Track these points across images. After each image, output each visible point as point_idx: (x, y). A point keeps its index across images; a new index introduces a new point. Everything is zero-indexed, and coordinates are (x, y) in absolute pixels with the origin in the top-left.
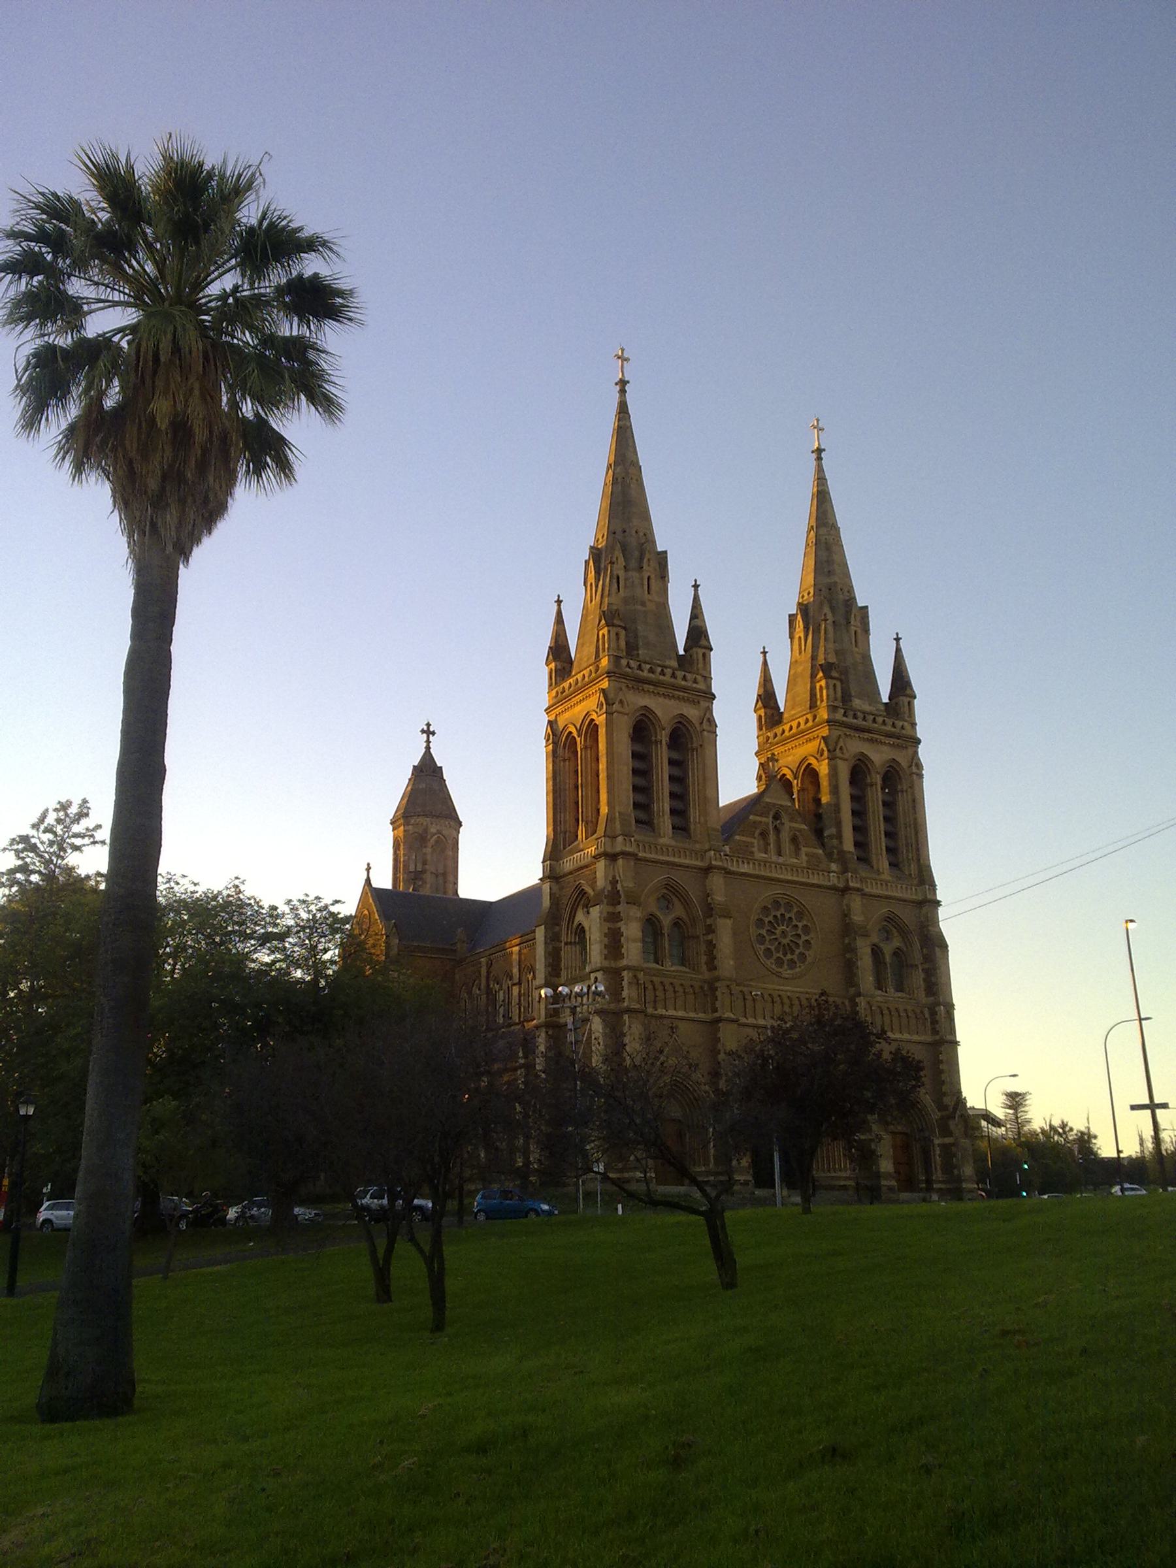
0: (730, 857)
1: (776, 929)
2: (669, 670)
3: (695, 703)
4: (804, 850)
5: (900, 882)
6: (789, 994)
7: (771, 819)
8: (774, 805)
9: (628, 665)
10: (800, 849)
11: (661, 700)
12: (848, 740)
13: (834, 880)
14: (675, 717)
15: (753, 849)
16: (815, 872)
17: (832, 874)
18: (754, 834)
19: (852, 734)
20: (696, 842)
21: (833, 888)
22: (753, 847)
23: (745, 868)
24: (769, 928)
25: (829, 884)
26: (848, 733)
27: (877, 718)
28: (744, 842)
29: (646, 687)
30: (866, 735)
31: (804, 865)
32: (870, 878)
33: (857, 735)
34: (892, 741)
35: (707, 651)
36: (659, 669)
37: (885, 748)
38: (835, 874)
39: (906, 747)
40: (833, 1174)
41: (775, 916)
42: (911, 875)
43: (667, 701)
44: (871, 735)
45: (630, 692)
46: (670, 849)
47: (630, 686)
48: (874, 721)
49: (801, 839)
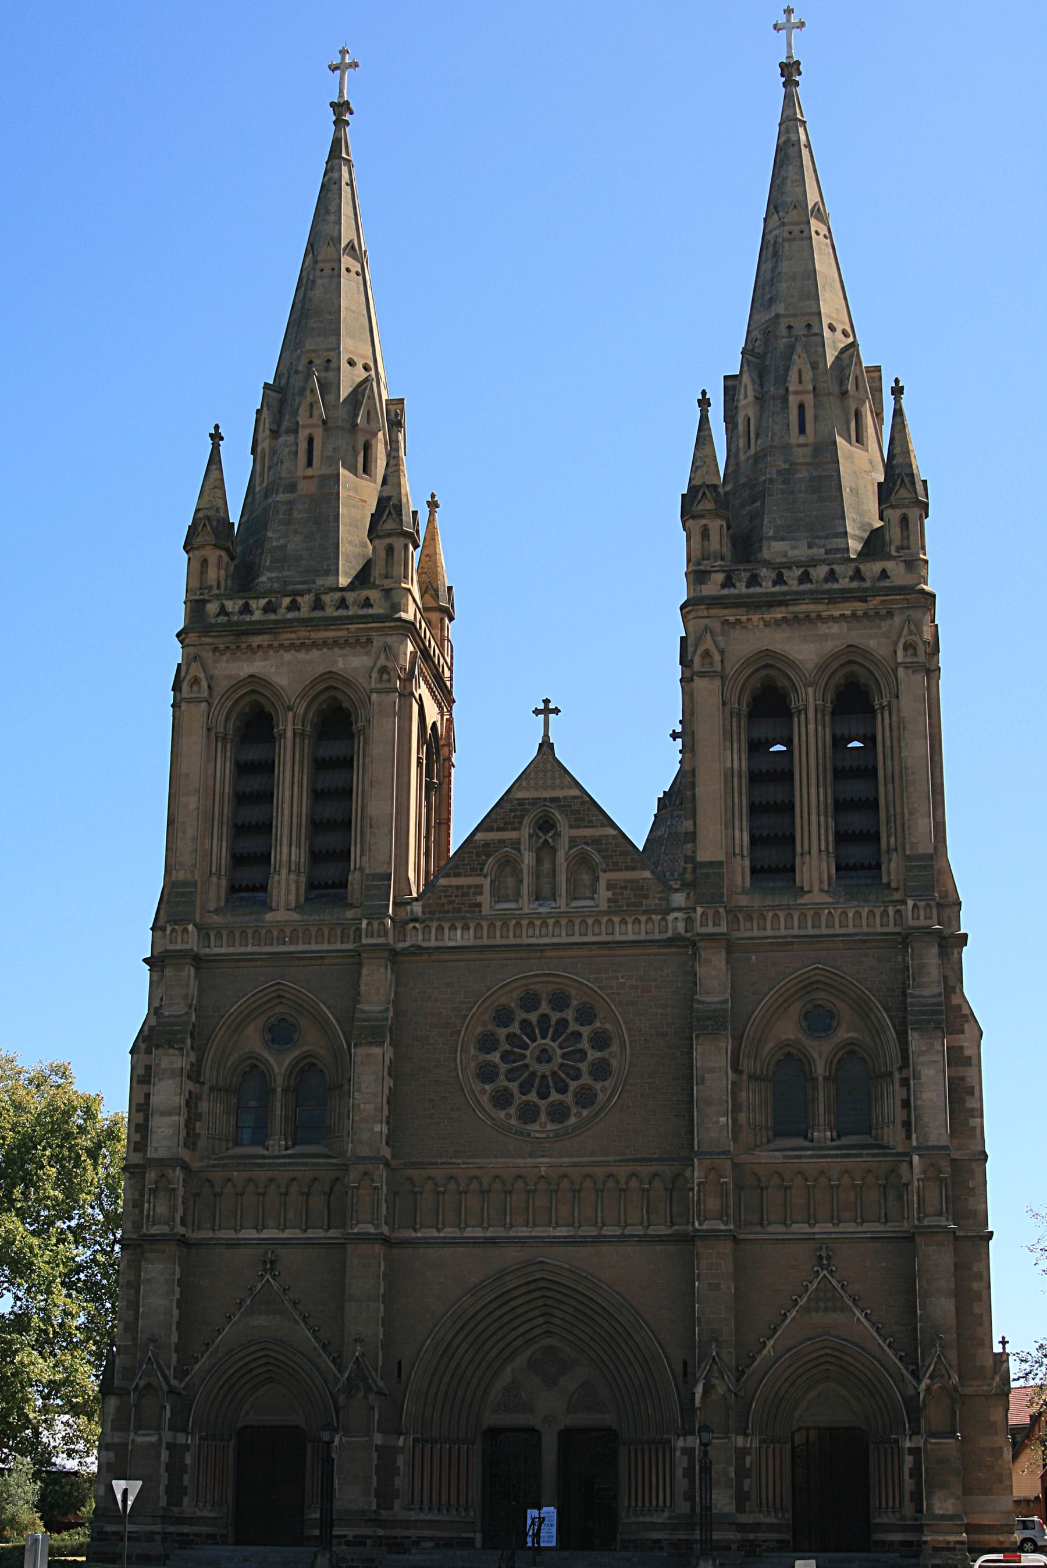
0: (423, 922)
1: (526, 1047)
2: (307, 597)
3: (361, 643)
4: (604, 878)
5: (855, 903)
6: (543, 1171)
7: (526, 831)
8: (535, 802)
9: (223, 611)
10: (597, 879)
11: (288, 656)
12: (737, 633)
13: (676, 923)
14: (313, 684)
15: (479, 899)
16: (630, 920)
17: (670, 917)
18: (482, 870)
19: (744, 618)
20: (351, 906)
21: (675, 941)
22: (481, 893)
23: (458, 938)
24: (508, 1048)
25: (665, 936)
26: (732, 619)
27: (811, 570)
28: (458, 887)
29: (256, 640)
30: (778, 613)
31: (603, 906)
32: (772, 907)
33: (755, 618)
34: (847, 608)
35: (398, 543)
36: (286, 601)
37: (835, 629)
38: (679, 915)
39: (890, 614)
40: (647, 1519)
41: (525, 1023)
42: (888, 885)
43: (302, 655)
44: (791, 609)
45: (224, 658)
46: (288, 931)
47: (222, 647)
48: (805, 578)
49: (597, 858)
